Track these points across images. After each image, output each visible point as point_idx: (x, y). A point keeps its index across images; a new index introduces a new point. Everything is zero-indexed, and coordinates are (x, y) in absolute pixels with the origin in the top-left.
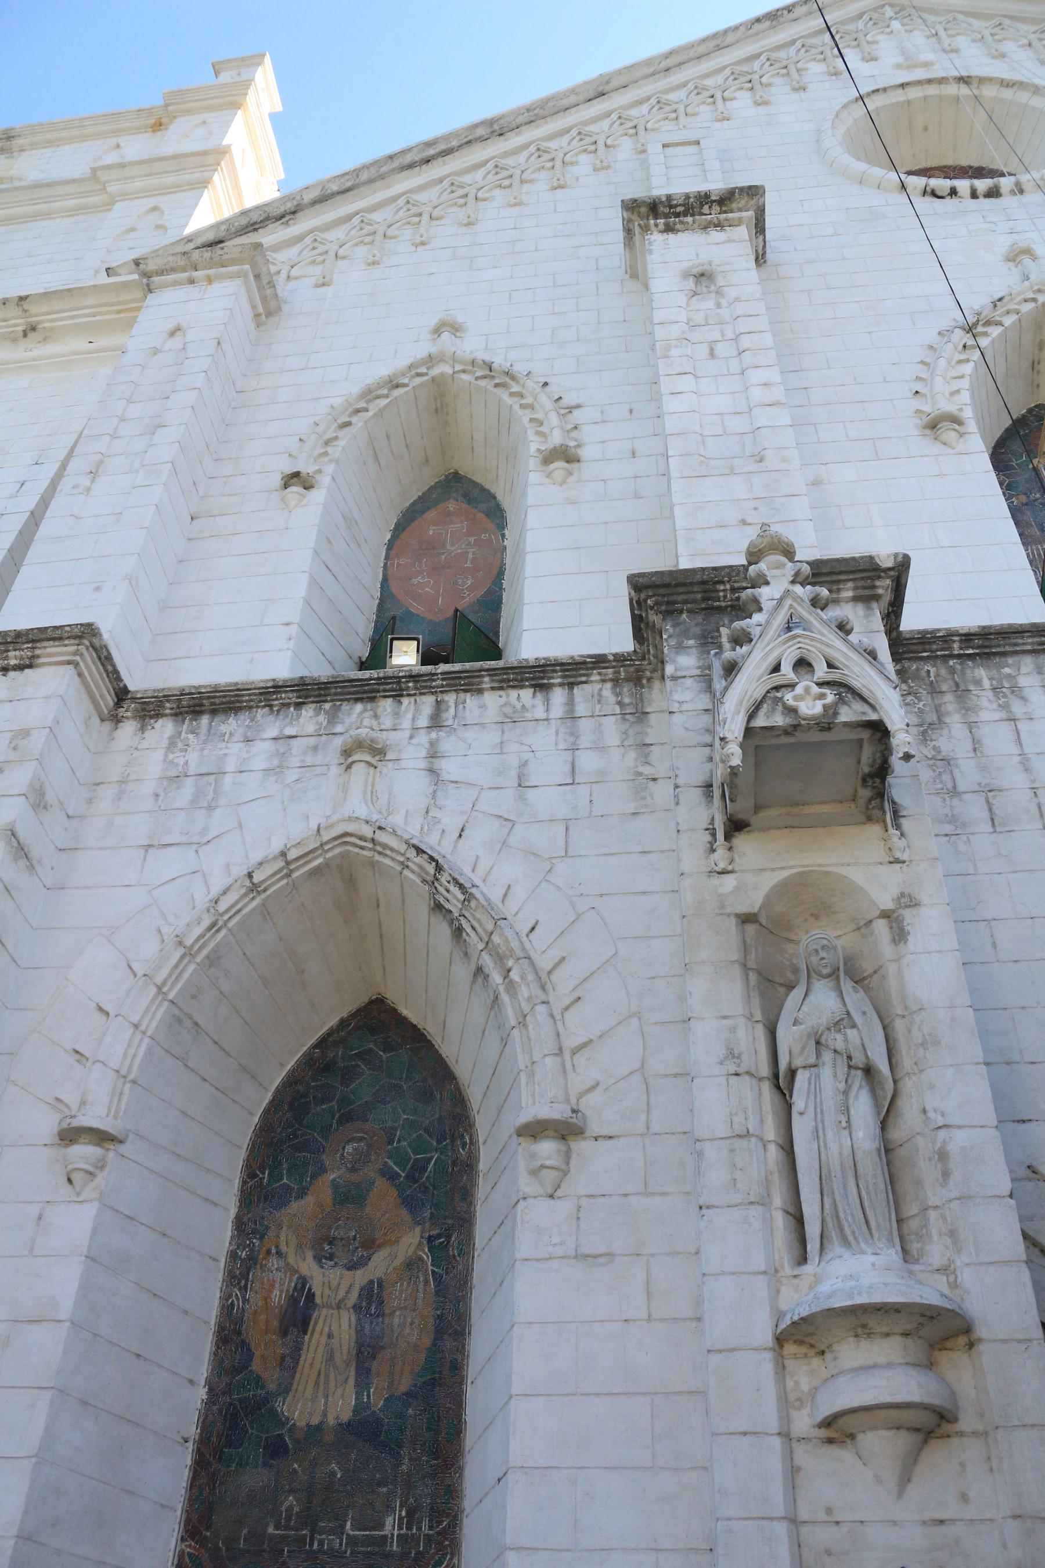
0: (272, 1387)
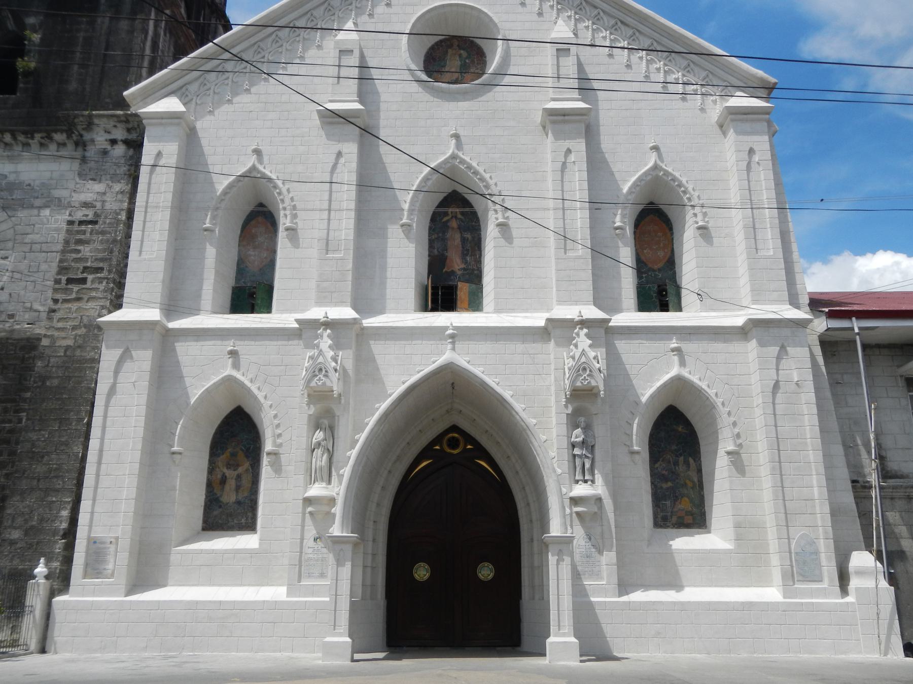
0: (218, 495)
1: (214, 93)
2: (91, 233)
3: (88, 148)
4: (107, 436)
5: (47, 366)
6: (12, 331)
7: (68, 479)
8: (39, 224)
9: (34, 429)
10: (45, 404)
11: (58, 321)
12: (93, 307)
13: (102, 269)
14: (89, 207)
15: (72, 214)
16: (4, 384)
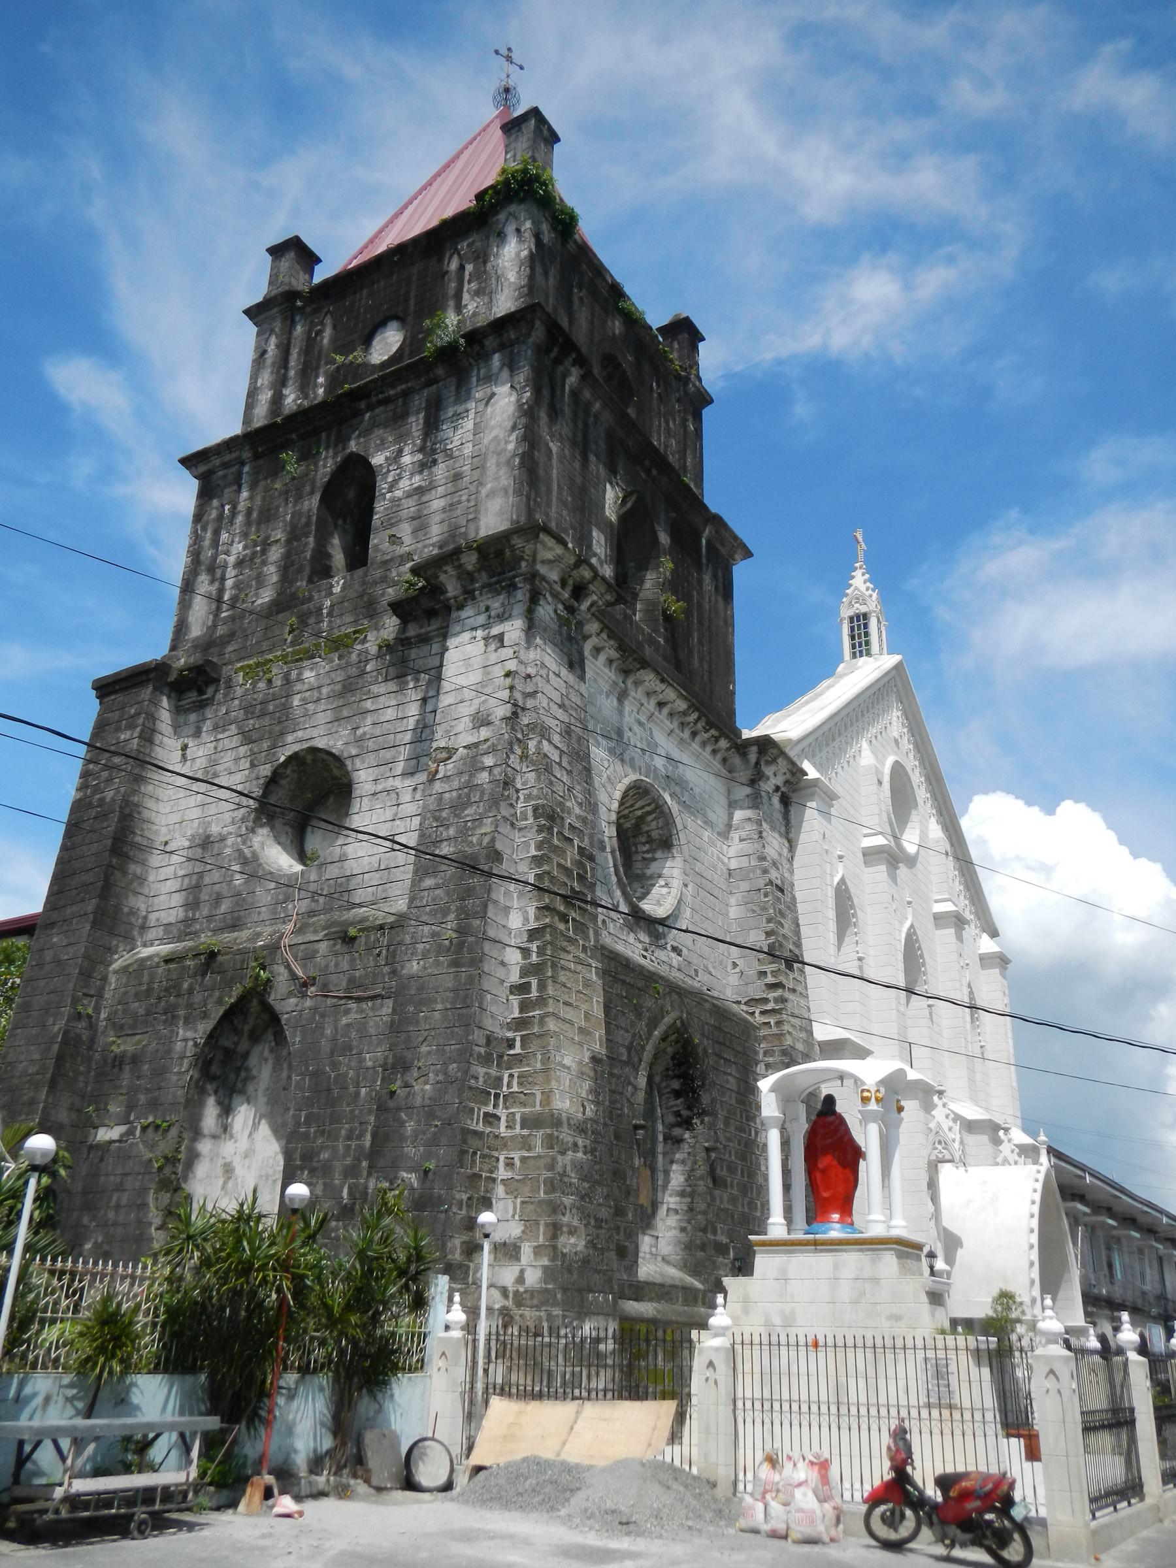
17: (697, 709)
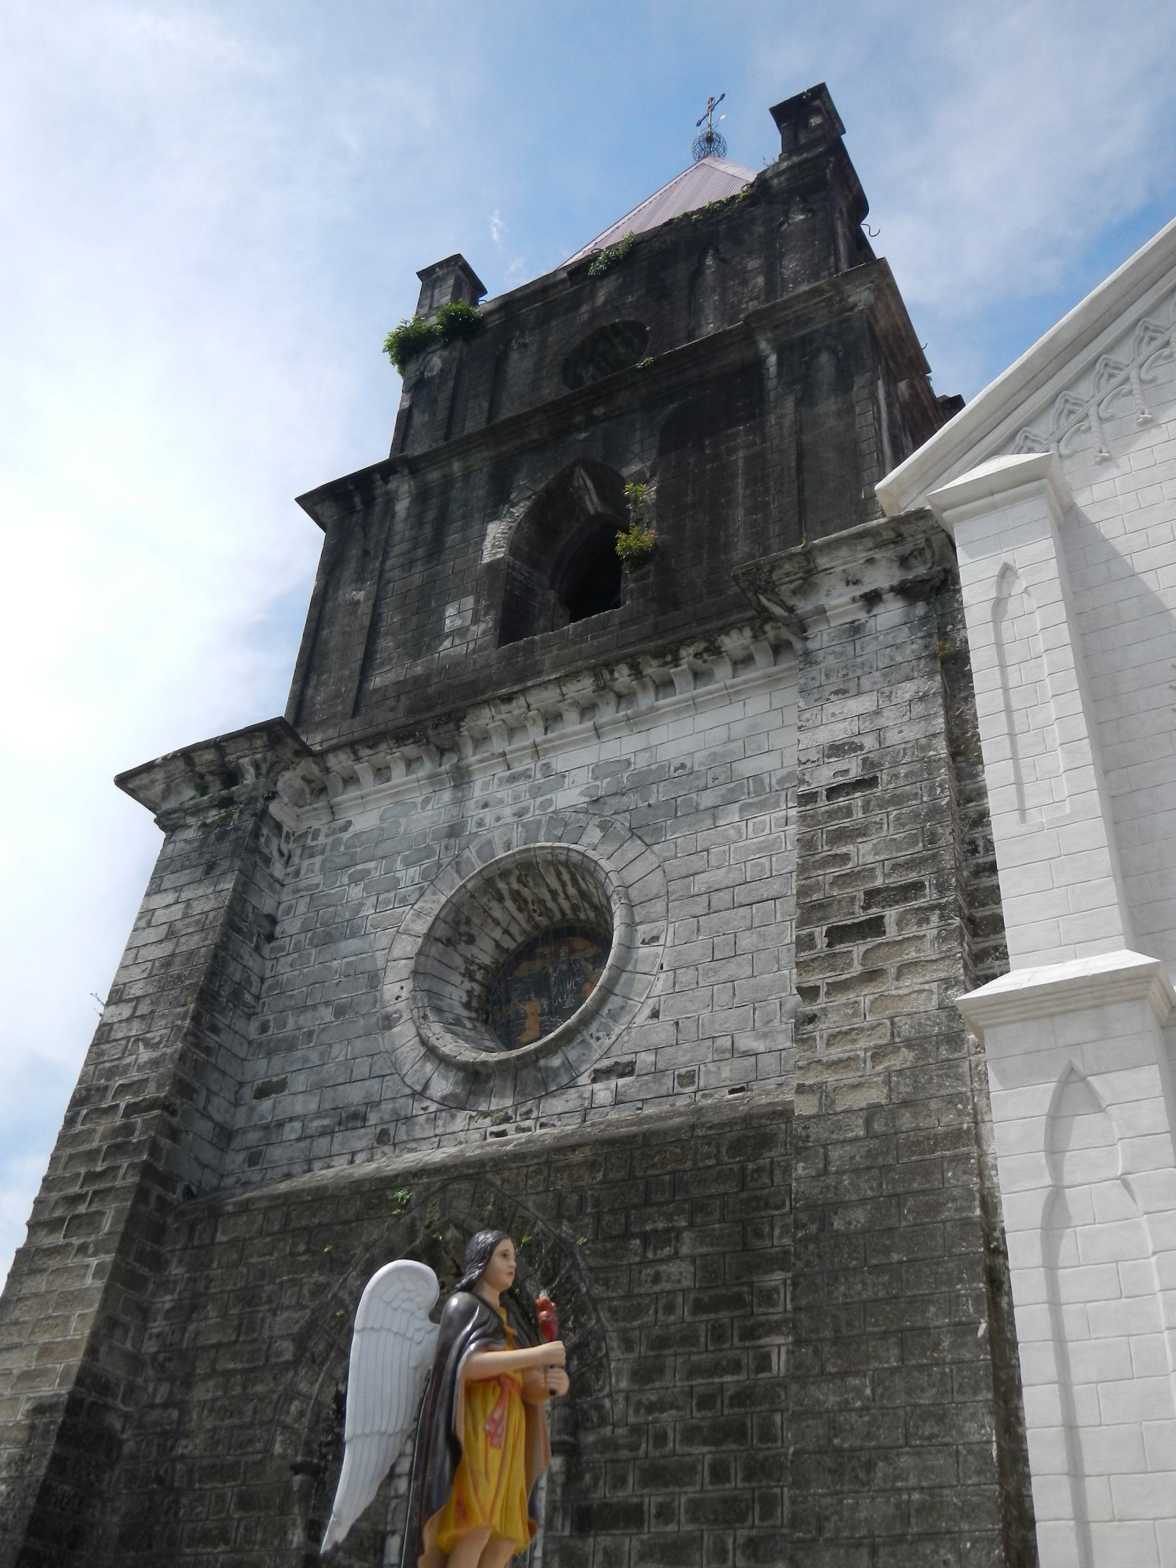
1: (1101, 420)
2: (866, 808)
3: (810, 633)
4: (1078, 1373)
5: (825, 1172)
6: (699, 1111)
7: (974, 1542)
8: (720, 845)
9: (822, 1372)
10: (842, 1289)
11: (828, 1044)
12: (917, 988)
13: (918, 887)
14: (845, 752)
15: (807, 778)
16: (703, 1256)
17: (610, 666)
